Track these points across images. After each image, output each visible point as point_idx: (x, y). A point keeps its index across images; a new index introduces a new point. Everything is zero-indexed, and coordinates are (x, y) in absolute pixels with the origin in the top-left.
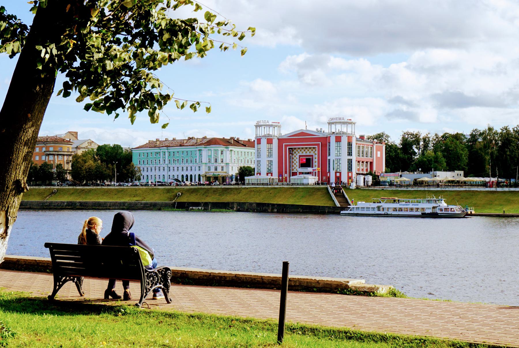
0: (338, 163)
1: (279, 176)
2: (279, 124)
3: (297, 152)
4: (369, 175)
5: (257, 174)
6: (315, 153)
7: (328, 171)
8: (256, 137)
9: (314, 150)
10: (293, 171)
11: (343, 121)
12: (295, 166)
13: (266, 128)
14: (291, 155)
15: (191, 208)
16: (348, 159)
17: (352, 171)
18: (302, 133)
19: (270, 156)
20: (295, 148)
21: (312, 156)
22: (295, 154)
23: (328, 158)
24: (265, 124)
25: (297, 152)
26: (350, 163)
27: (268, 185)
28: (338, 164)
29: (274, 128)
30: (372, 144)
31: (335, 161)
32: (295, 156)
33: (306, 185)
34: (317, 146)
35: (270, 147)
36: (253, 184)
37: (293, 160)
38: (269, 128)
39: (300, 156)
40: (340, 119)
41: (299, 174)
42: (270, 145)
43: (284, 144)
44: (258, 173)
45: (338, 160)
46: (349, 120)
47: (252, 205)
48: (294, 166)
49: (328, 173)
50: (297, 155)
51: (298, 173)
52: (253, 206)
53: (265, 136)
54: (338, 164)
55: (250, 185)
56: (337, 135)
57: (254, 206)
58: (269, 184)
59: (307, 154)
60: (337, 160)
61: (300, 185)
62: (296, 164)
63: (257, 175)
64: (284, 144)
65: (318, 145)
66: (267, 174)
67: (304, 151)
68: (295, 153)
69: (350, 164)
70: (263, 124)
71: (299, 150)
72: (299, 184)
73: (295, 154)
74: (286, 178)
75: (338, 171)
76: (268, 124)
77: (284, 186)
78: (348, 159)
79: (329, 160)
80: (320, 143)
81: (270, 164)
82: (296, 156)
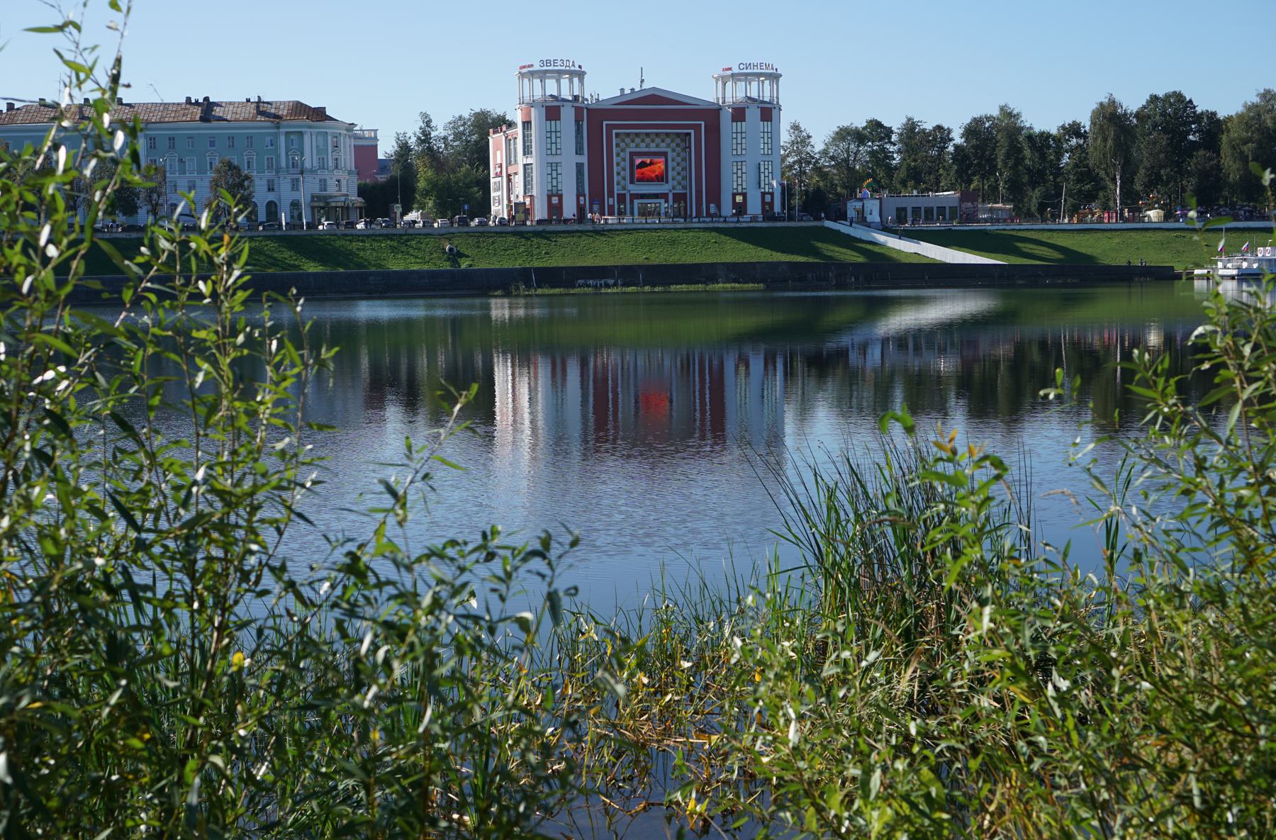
15: (581, 282)
18: (653, 95)
21: (665, 154)
34: (692, 132)
40: (767, 66)
50: (623, 150)
67: (643, 141)
71: (628, 140)
82: (622, 154)
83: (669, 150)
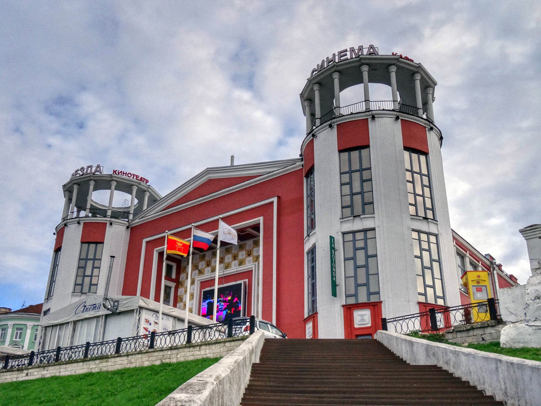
0: (361, 255)
14: (173, 285)
28: (361, 261)
31: (339, 245)
34: (261, 219)
35: (91, 256)
54: (361, 261)
59: (229, 271)
64: (144, 241)
65: (266, 210)
75: (363, 298)
80: (275, 200)
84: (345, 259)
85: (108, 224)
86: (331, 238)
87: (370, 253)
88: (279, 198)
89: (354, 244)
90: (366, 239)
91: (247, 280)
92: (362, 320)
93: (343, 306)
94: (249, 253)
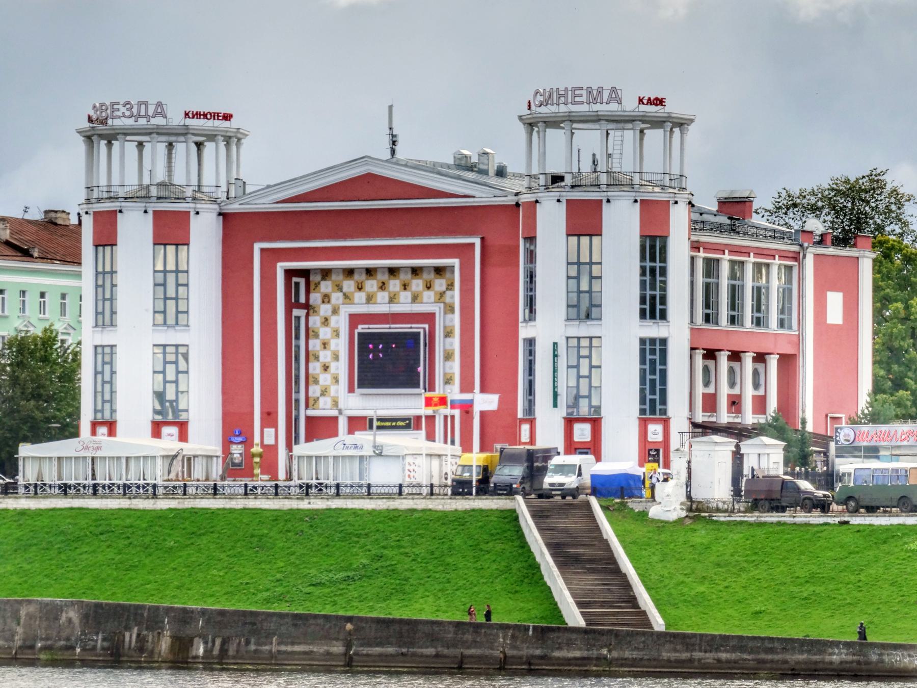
1: (227, 443)
2: (226, 124)
3: (337, 298)
4: (766, 440)
5: (95, 425)
6: (447, 299)
7: (520, 415)
8: (88, 201)
9: (440, 284)
10: (311, 413)
11: (614, 107)
12: (325, 379)
13: (148, 147)
14: (301, 313)
16: (643, 341)
17: (664, 412)
18: (369, 178)
19: (171, 320)
20: (326, 273)
21: (429, 318)
22: (325, 310)
23: (525, 332)
24: (142, 122)
25: (337, 298)
26: (653, 362)
27: (155, 496)
28: (584, 371)
29: (199, 145)
30: (795, 248)
31: (562, 351)
32: (326, 321)
33: (389, 496)
34: (456, 262)
35: (171, 266)
36: (65, 489)
37: (315, 344)
38: (170, 145)
39: (355, 319)
40: (595, 96)
41: (351, 431)
42: (171, 249)
43: (257, 247)
44: (103, 423)
45: (586, 343)
46: (650, 102)
47: (57, 618)
48: (316, 382)
49: (522, 421)
50: (335, 311)
51: (343, 424)
52: (63, 618)
53: (142, 196)
54: (584, 371)
55: (51, 496)
56: (577, 195)
57: (70, 620)
58: (161, 491)
59: (397, 309)
60: (574, 342)
61: (352, 496)
62: (333, 366)
63: (94, 433)
64: (257, 247)
66: (156, 429)
67: (383, 286)
68: (326, 298)
69: (653, 372)
70: (131, 122)
71: (349, 285)
72: (344, 490)
73: (325, 310)
74: (270, 451)
75: (584, 410)
76: (159, 121)
77: (252, 503)
78: (643, 341)
79: (531, 343)
80: (477, 241)
81: (171, 369)
82: (333, 320)
83: (437, 309)
84: (569, 367)
85: (192, 214)
86: (555, 344)
87: (594, 363)
88: (483, 239)
89: (579, 352)
90: (591, 347)
91: (426, 326)
92: (583, 434)
93: (564, 418)
94: (428, 285)
